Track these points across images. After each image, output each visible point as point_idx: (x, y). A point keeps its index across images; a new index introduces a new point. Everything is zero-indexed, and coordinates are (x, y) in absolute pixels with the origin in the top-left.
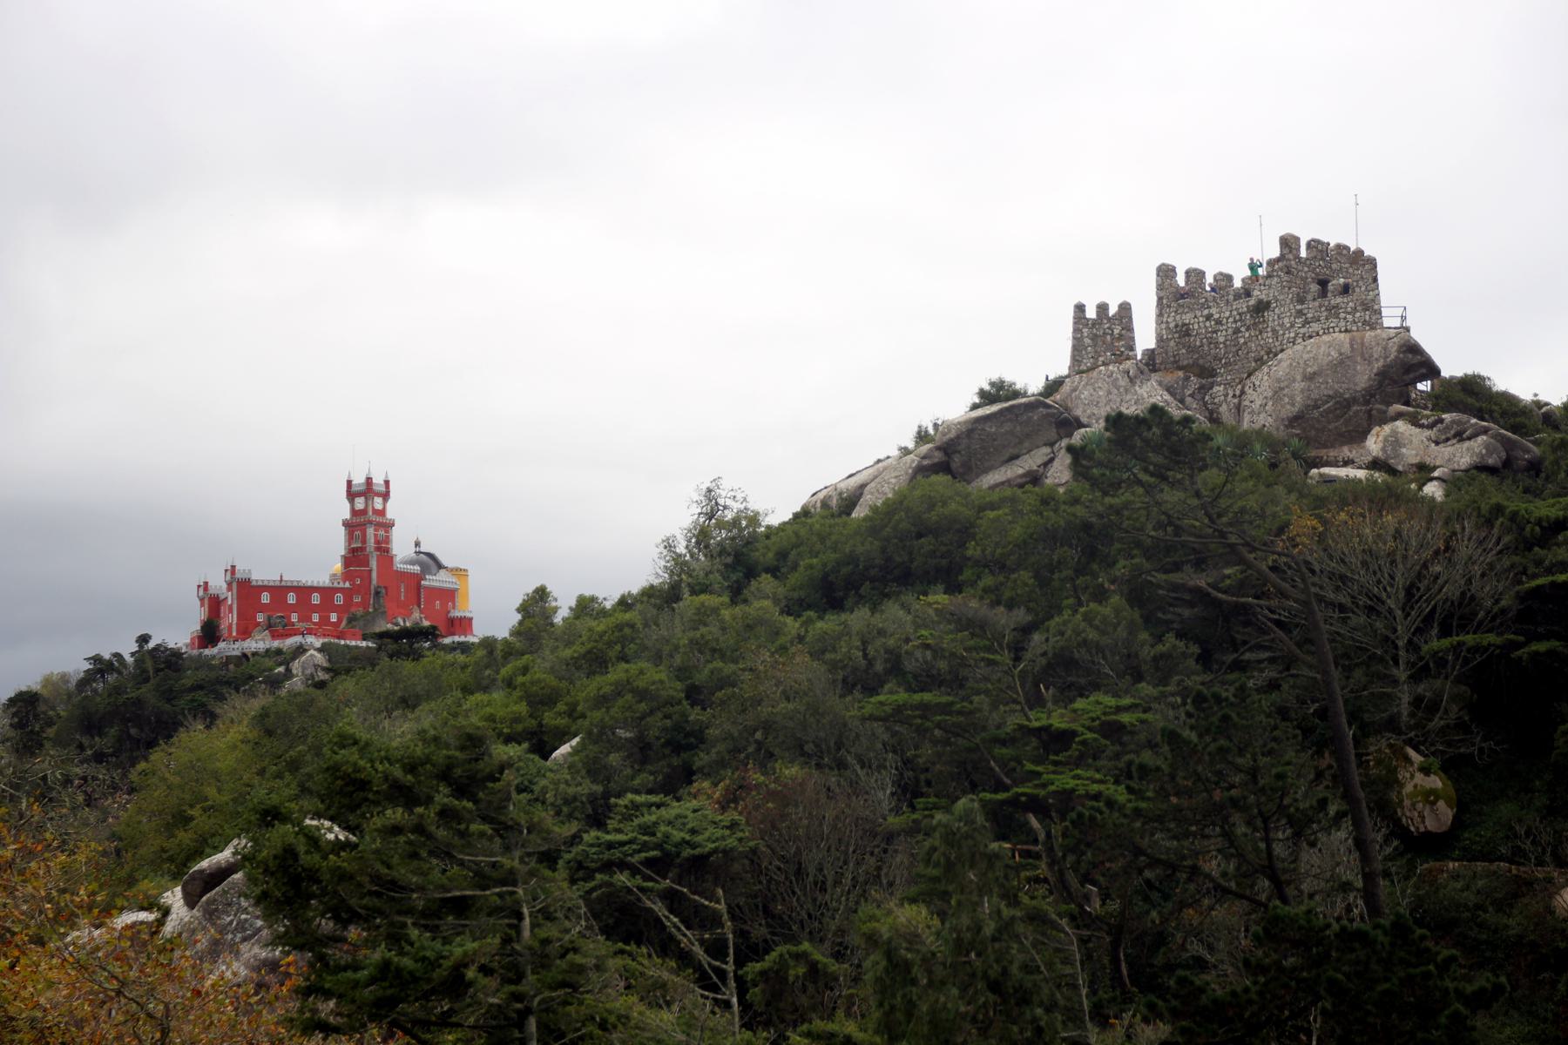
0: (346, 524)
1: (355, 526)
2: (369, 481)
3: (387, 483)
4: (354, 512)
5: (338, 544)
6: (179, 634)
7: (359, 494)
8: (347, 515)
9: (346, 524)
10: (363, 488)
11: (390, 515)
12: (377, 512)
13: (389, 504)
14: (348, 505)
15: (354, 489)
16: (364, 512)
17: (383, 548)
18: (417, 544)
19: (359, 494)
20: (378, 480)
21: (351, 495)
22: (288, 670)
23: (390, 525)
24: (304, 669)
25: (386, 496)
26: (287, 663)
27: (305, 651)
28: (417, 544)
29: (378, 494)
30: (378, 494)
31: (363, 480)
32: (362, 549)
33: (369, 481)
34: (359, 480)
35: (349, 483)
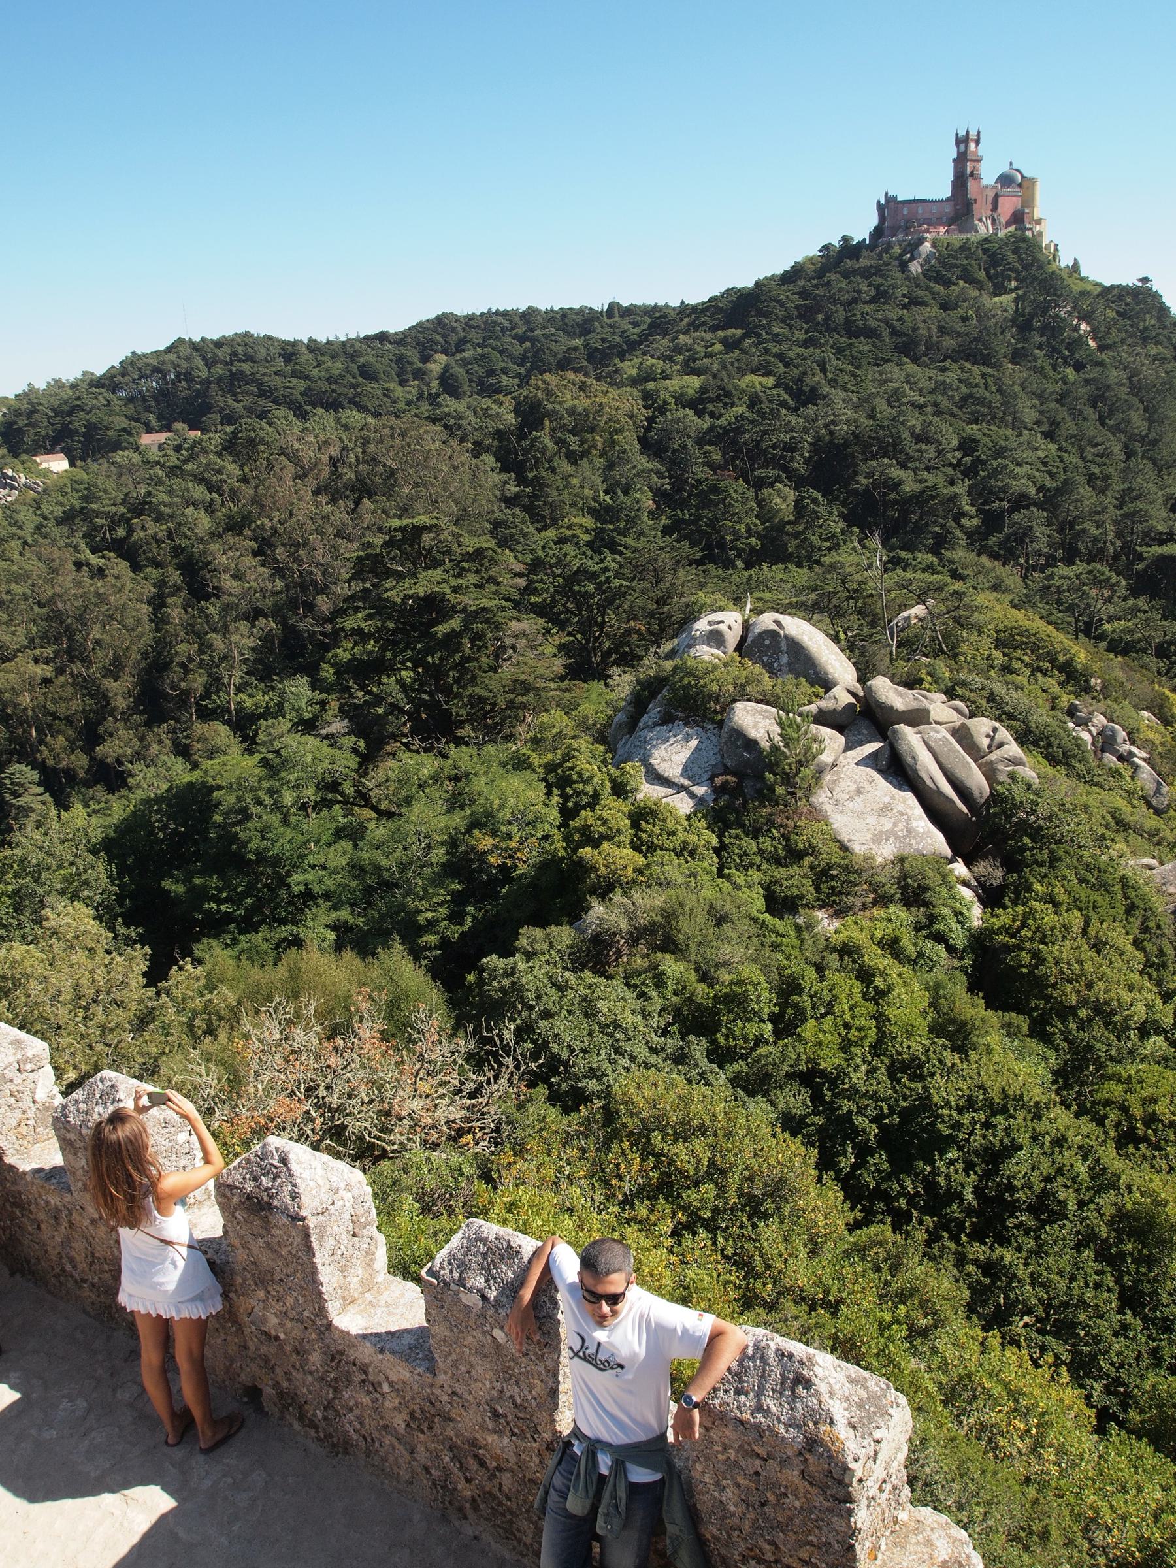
1: (961, 160)
4: (959, 153)
6: (861, 232)
17: (974, 175)
20: (973, 134)
25: (977, 142)
34: (962, 133)
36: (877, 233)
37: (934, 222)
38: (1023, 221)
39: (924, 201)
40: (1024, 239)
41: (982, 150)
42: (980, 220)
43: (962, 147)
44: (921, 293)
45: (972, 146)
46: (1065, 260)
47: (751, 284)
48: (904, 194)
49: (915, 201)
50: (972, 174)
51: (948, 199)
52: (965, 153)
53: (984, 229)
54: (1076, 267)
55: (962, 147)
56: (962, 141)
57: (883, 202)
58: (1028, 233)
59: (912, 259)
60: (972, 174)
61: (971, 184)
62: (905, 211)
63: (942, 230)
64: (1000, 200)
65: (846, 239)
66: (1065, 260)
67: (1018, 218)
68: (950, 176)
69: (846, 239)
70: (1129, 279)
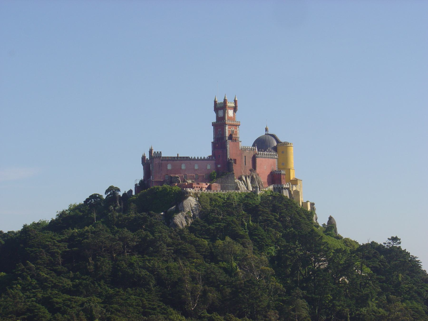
1: (219, 125)
2: (225, 101)
3: (235, 102)
4: (218, 118)
5: (209, 136)
8: (215, 120)
9: (213, 124)
10: (222, 105)
14: (214, 115)
15: (218, 106)
25: (235, 109)
29: (230, 108)
30: (230, 108)
31: (222, 101)
33: (225, 101)
34: (220, 100)
35: (215, 102)
37: (198, 179)
38: (280, 182)
39: (187, 159)
40: (282, 198)
41: (240, 117)
42: (240, 179)
43: (221, 113)
44: (187, 246)
45: (230, 113)
46: (322, 220)
47: (17, 228)
48: (167, 152)
50: (231, 137)
51: (210, 158)
52: (223, 118)
53: (244, 187)
54: (331, 225)
56: (220, 108)
57: (147, 157)
58: (286, 193)
59: (177, 211)
60: (231, 137)
61: (229, 145)
62: (169, 167)
63: (205, 186)
66: (322, 220)
67: (275, 178)
68: (211, 139)
69: (112, 191)
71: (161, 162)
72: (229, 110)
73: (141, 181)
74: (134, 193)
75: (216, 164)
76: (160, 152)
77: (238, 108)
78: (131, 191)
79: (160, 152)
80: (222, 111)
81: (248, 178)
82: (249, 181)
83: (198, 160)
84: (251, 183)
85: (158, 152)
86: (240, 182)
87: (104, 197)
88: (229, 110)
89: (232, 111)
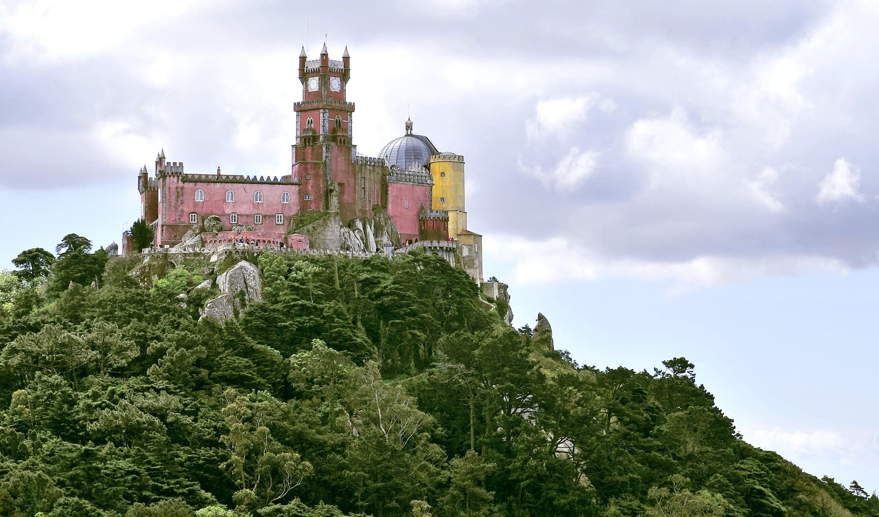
0: (298, 108)
2: (324, 56)
3: (346, 59)
4: (306, 92)
5: (288, 133)
7: (314, 73)
11: (348, 100)
12: (331, 94)
13: (349, 86)
14: (300, 87)
15: (310, 67)
16: (317, 94)
18: (409, 127)
19: (314, 73)
20: (336, 56)
21: (304, 75)
22: (214, 285)
23: (351, 108)
24: (231, 284)
25: (344, 75)
26: (213, 275)
27: (235, 261)
28: (409, 127)
29: (336, 73)
30: (336, 73)
31: (318, 57)
32: (315, 138)
33: (324, 56)
34: (314, 56)
35: (303, 59)
36: (140, 236)
43: (314, 84)
45: (335, 84)
49: (219, 179)
51: (286, 181)
55: (314, 84)
62: (199, 198)
64: (392, 191)
65: (74, 242)
69: (74, 242)
70: (647, 360)
71: (181, 184)
72: (332, 78)
73: (136, 225)
74: (120, 252)
75: (302, 194)
76: (181, 164)
77: (352, 73)
78: (115, 247)
79: (181, 164)
80: (317, 78)
81: (368, 226)
82: (370, 232)
83: (262, 182)
84: (376, 235)
85: (175, 163)
86: (351, 232)
87: (56, 256)
88: (332, 78)
89: (338, 79)
